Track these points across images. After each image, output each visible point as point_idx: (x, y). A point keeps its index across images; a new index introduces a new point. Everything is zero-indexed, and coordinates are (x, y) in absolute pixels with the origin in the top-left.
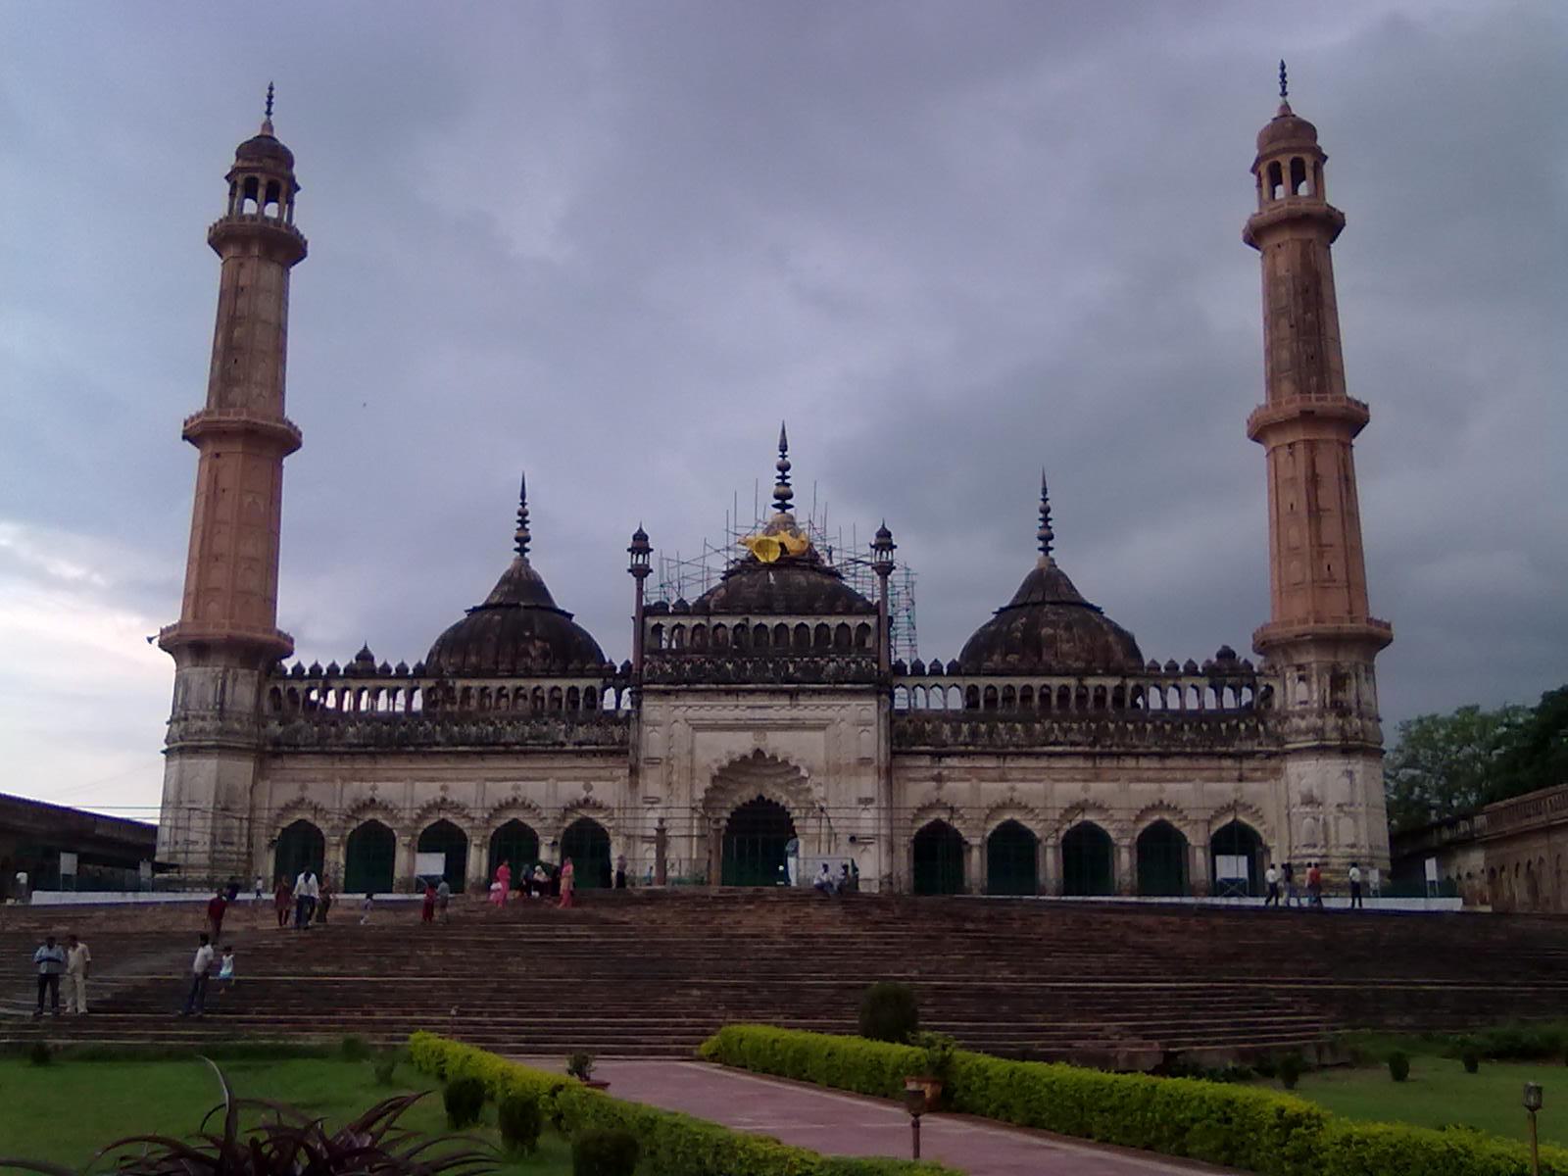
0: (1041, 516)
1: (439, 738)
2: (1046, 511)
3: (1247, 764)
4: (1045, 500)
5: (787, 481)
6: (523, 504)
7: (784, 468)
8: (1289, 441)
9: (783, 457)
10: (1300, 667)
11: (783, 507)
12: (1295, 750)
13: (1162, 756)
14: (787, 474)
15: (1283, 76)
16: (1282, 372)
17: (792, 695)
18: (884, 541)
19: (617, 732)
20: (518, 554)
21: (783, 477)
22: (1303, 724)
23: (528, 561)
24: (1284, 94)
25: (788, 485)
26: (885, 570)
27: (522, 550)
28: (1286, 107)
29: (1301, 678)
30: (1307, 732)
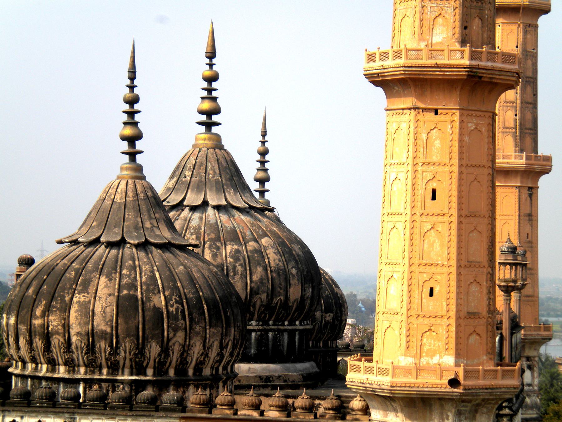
0: (259, 157)
2: (264, 153)
4: (263, 143)
5: (214, 94)
6: (132, 87)
7: (212, 79)
8: (530, 185)
9: (211, 65)
10: (528, 359)
11: (209, 125)
14: (215, 85)
16: (526, 129)
21: (210, 91)
23: (140, 168)
25: (214, 99)
27: (133, 155)
29: (530, 367)
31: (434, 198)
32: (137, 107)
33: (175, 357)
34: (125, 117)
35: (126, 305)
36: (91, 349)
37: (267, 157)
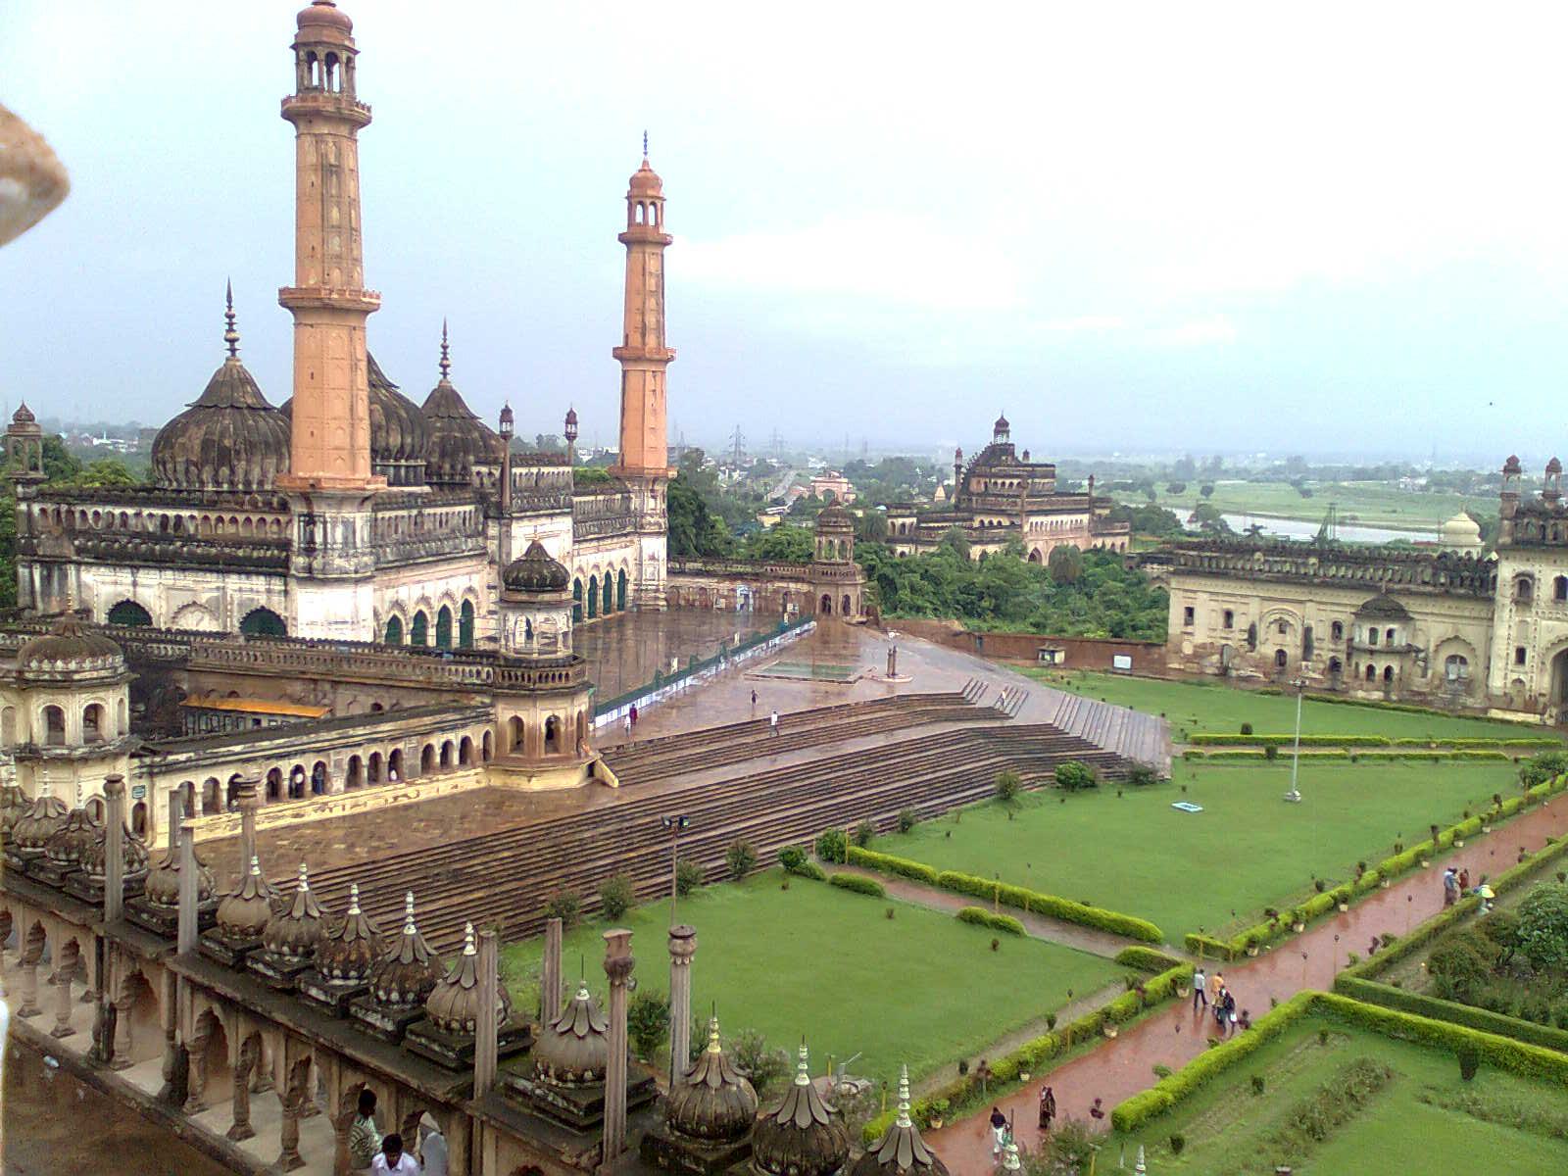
0: (442, 350)
1: (423, 553)
2: (445, 347)
3: (629, 538)
6: (230, 307)
12: (650, 534)
13: (612, 537)
15: (646, 141)
17: (551, 516)
18: (571, 419)
19: (480, 539)
20: (229, 353)
22: (652, 520)
24: (646, 153)
26: (571, 437)
28: (645, 163)
29: (653, 497)
30: (655, 524)
31: (312, 378)
32: (234, 320)
33: (240, 476)
34: (227, 327)
35: (206, 445)
36: (187, 471)
37: (448, 350)
